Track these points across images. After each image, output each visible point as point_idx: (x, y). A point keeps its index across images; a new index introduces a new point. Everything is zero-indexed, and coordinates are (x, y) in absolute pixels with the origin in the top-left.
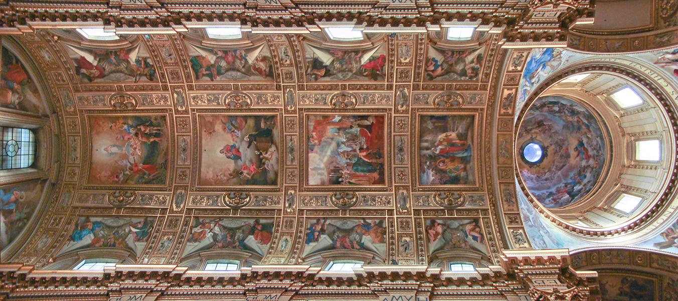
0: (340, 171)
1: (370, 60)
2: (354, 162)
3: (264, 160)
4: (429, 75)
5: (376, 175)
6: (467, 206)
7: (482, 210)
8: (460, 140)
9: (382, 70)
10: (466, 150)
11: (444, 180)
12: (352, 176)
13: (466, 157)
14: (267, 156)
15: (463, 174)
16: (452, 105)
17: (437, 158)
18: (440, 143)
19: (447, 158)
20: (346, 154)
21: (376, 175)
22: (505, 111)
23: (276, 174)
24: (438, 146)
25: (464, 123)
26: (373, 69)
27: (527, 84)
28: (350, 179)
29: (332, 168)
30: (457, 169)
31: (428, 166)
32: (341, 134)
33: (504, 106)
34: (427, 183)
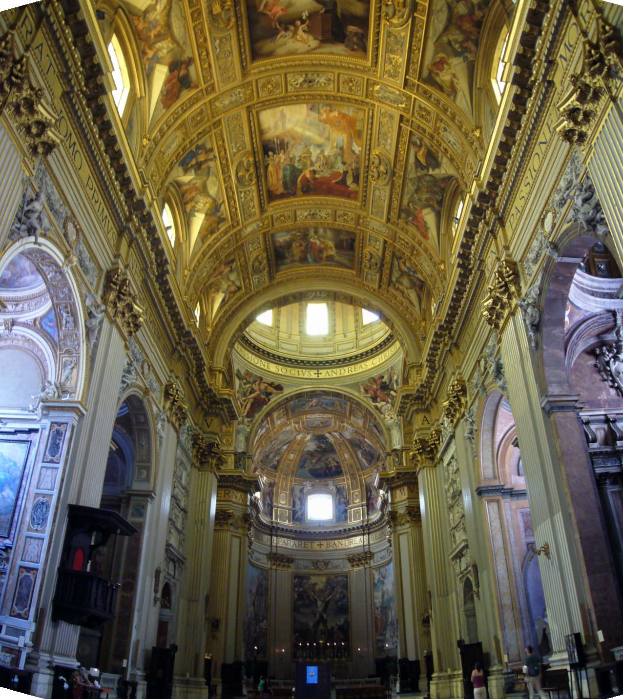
0: (282, 151)
1: (425, 223)
2: (296, 165)
3: (292, 28)
4: (401, 258)
5: (281, 190)
9: (413, 224)
12: (277, 167)
14: (300, 32)
15: (288, 261)
18: (322, 242)
19: (305, 248)
20: (307, 155)
21: (281, 190)
23: (270, 54)
26: (415, 216)
28: (274, 164)
29: (286, 140)
30: (293, 255)
31: (294, 235)
32: (335, 149)
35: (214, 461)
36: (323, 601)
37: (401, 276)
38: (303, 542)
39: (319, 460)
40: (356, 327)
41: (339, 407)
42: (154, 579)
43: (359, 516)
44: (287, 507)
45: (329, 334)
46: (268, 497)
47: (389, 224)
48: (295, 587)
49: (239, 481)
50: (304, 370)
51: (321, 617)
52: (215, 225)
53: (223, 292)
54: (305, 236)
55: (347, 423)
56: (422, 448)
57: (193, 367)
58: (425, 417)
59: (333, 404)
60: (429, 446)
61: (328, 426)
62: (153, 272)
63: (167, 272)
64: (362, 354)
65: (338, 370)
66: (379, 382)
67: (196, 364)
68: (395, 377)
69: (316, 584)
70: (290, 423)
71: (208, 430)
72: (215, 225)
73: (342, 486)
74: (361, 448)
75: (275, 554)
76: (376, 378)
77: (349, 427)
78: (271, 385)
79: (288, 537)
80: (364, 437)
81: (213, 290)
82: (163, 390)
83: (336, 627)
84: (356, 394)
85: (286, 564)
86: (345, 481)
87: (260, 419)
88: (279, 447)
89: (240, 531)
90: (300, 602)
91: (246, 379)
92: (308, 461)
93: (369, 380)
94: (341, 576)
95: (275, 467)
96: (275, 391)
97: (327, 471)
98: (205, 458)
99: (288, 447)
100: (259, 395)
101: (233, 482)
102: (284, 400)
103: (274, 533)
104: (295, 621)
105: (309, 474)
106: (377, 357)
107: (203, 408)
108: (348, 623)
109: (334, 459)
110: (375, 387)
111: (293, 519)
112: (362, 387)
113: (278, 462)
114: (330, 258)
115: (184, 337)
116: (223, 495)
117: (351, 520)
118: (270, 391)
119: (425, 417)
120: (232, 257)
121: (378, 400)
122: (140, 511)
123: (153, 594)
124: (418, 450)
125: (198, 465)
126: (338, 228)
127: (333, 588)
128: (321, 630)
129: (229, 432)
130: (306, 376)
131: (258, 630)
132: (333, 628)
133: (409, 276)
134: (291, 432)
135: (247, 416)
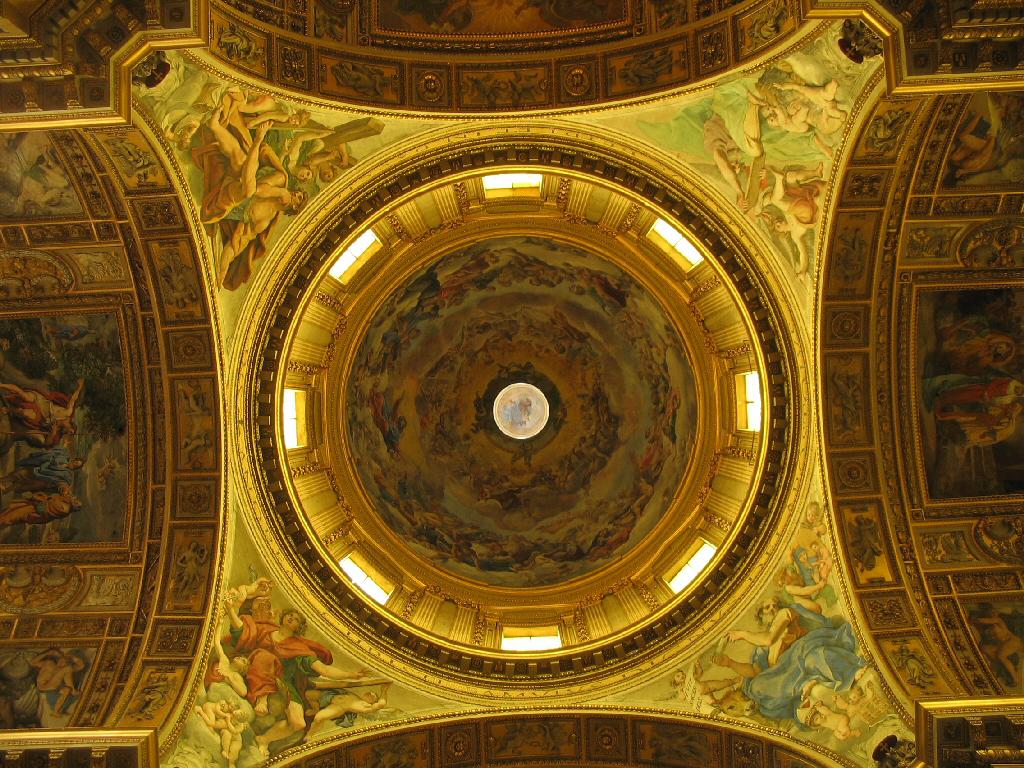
6: (960, 225)
7: (925, 214)
8: (955, 424)
10: (936, 393)
13: (936, 374)
15: (948, 322)
16: (1008, 525)
18: (1007, 411)
22: (865, 515)
24: (1013, 404)
27: (806, 604)
33: (873, 532)
41: (26, 511)
66: (300, 649)
68: (359, 706)
76: (309, 636)
78: (258, 246)
84: (226, 575)
91: (323, 153)
93: (291, 611)
96: (231, 255)
100: (242, 189)
112: (253, 587)
114: (950, 433)
118: (236, 238)
121: (241, 661)
135: (205, 130)
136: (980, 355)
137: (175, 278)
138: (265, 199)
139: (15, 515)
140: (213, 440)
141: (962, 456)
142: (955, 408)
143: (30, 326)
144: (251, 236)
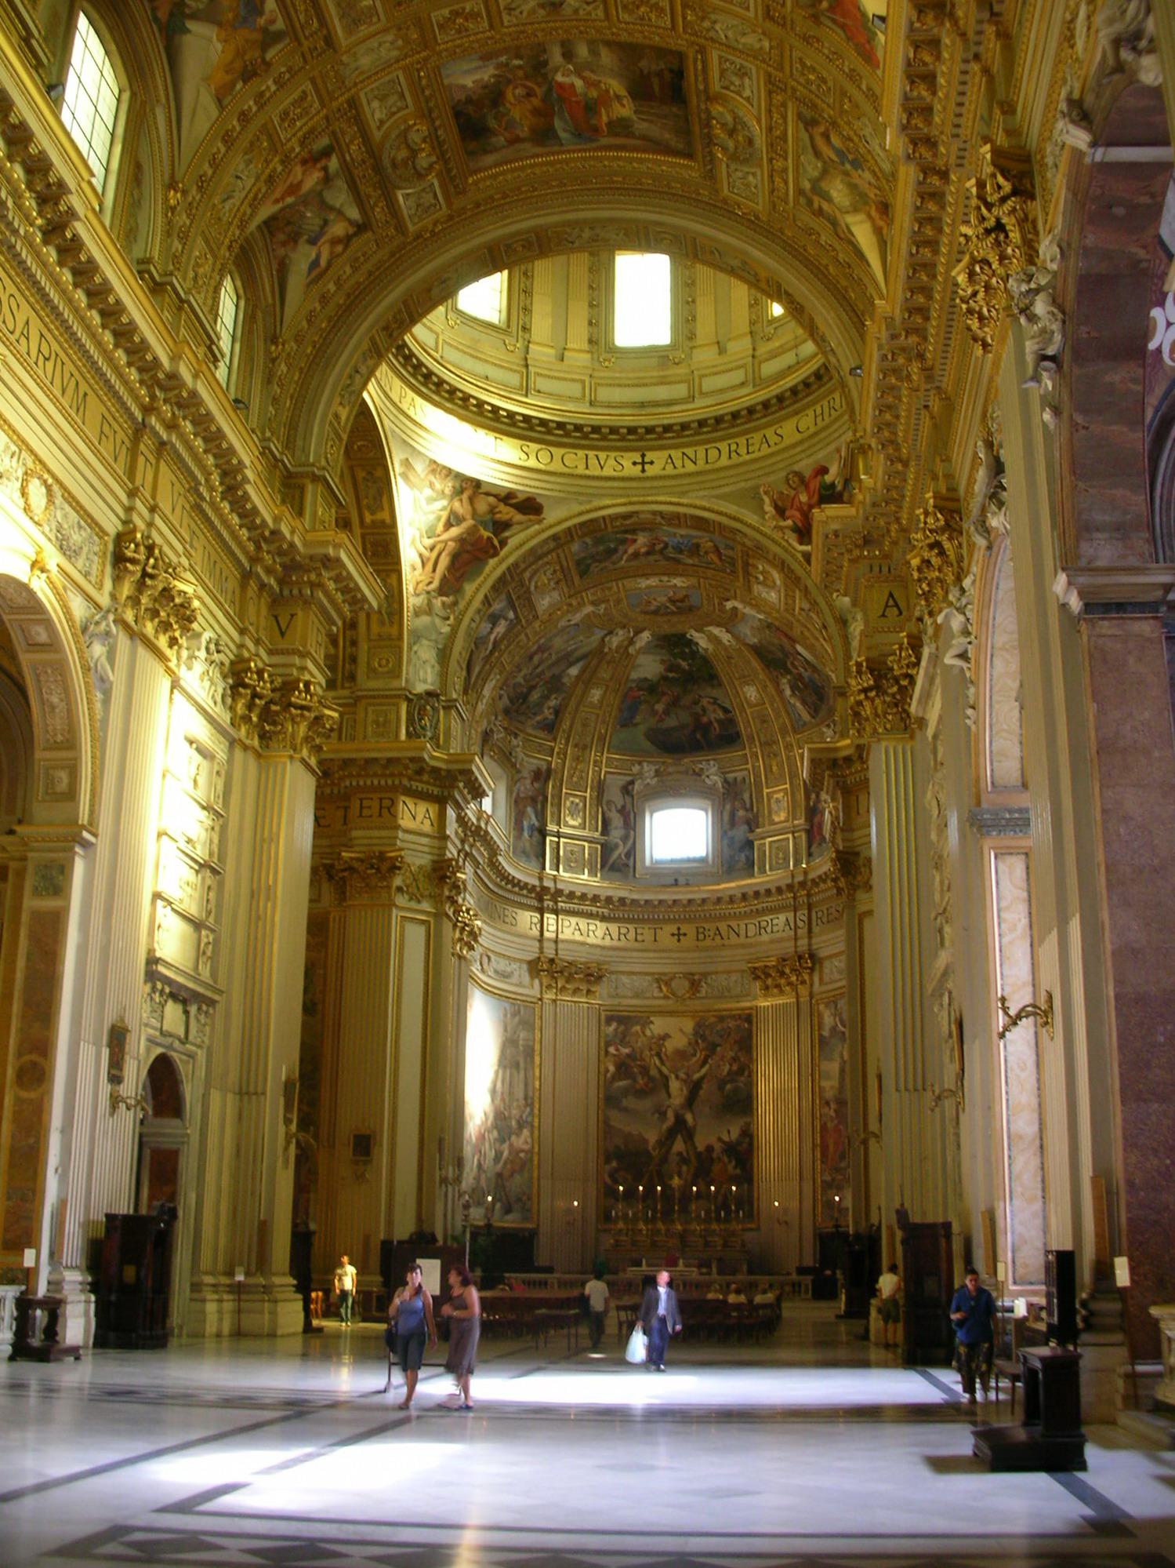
8: (610, 124)
9: (834, 21)
11: (470, 109)
13: (557, 137)
15: (500, 140)
17: (540, 80)
19: (544, 101)
25: (667, 136)
31: (507, 65)
34: (448, 76)
35: (302, 729)
36: (685, 1081)
37: (825, 172)
38: (631, 927)
39: (675, 703)
40: (752, 323)
41: (713, 557)
42: (105, 1053)
43: (786, 859)
44: (586, 833)
45: (674, 346)
46: (529, 810)
47: (769, 25)
48: (608, 1044)
49: (420, 772)
50: (602, 455)
51: (680, 1121)
52: (253, 54)
53: (313, 242)
54: (539, 67)
55: (743, 601)
56: (877, 687)
57: (208, 474)
58: (891, 595)
59: (695, 549)
60: (897, 681)
61: (691, 609)
62: (27, 217)
63: (72, 213)
64: (766, 405)
65: (701, 450)
66: (815, 484)
67: (217, 466)
69: (666, 1037)
70: (581, 605)
71: (283, 645)
72: (253, 54)
73: (739, 775)
74: (788, 672)
75: (552, 961)
76: (807, 473)
77: (748, 610)
79: (590, 916)
80: (793, 640)
81: (281, 237)
82: (111, 547)
83: (718, 1147)
84: (752, 518)
85: (584, 987)
86: (748, 763)
87: (480, 596)
88: (556, 670)
89: (426, 906)
90: (621, 1083)
92: (643, 707)
93: (787, 480)
94: (733, 1017)
95: (550, 727)
96: (519, 517)
97: (698, 736)
98: (274, 723)
99: (583, 671)
100: (471, 531)
101: (401, 775)
102: (545, 541)
103: (548, 903)
104: (607, 1129)
105: (647, 744)
106: (811, 412)
107: (262, 586)
108: (751, 1137)
109: (715, 701)
110: (804, 498)
111: (602, 867)
112: (767, 500)
113: (557, 712)
114: (620, 127)
115: (162, 388)
116: (375, 811)
117: (763, 871)
119: (891, 595)
120: (324, 141)
122: (56, 881)
123: (105, 1088)
124: (865, 691)
125: (256, 742)
126: (630, 40)
127: (712, 1048)
128: (680, 1154)
129: (390, 638)
130: (608, 472)
131: (506, 1154)
132: (710, 1149)
133: (847, 174)
134: (588, 624)
136: (529, 107)
137: (540, 551)
138: (474, 510)
139: (715, 559)
140: (654, 513)
141: (645, 125)
142: (593, 122)
143: (578, 563)
144: (502, 507)
